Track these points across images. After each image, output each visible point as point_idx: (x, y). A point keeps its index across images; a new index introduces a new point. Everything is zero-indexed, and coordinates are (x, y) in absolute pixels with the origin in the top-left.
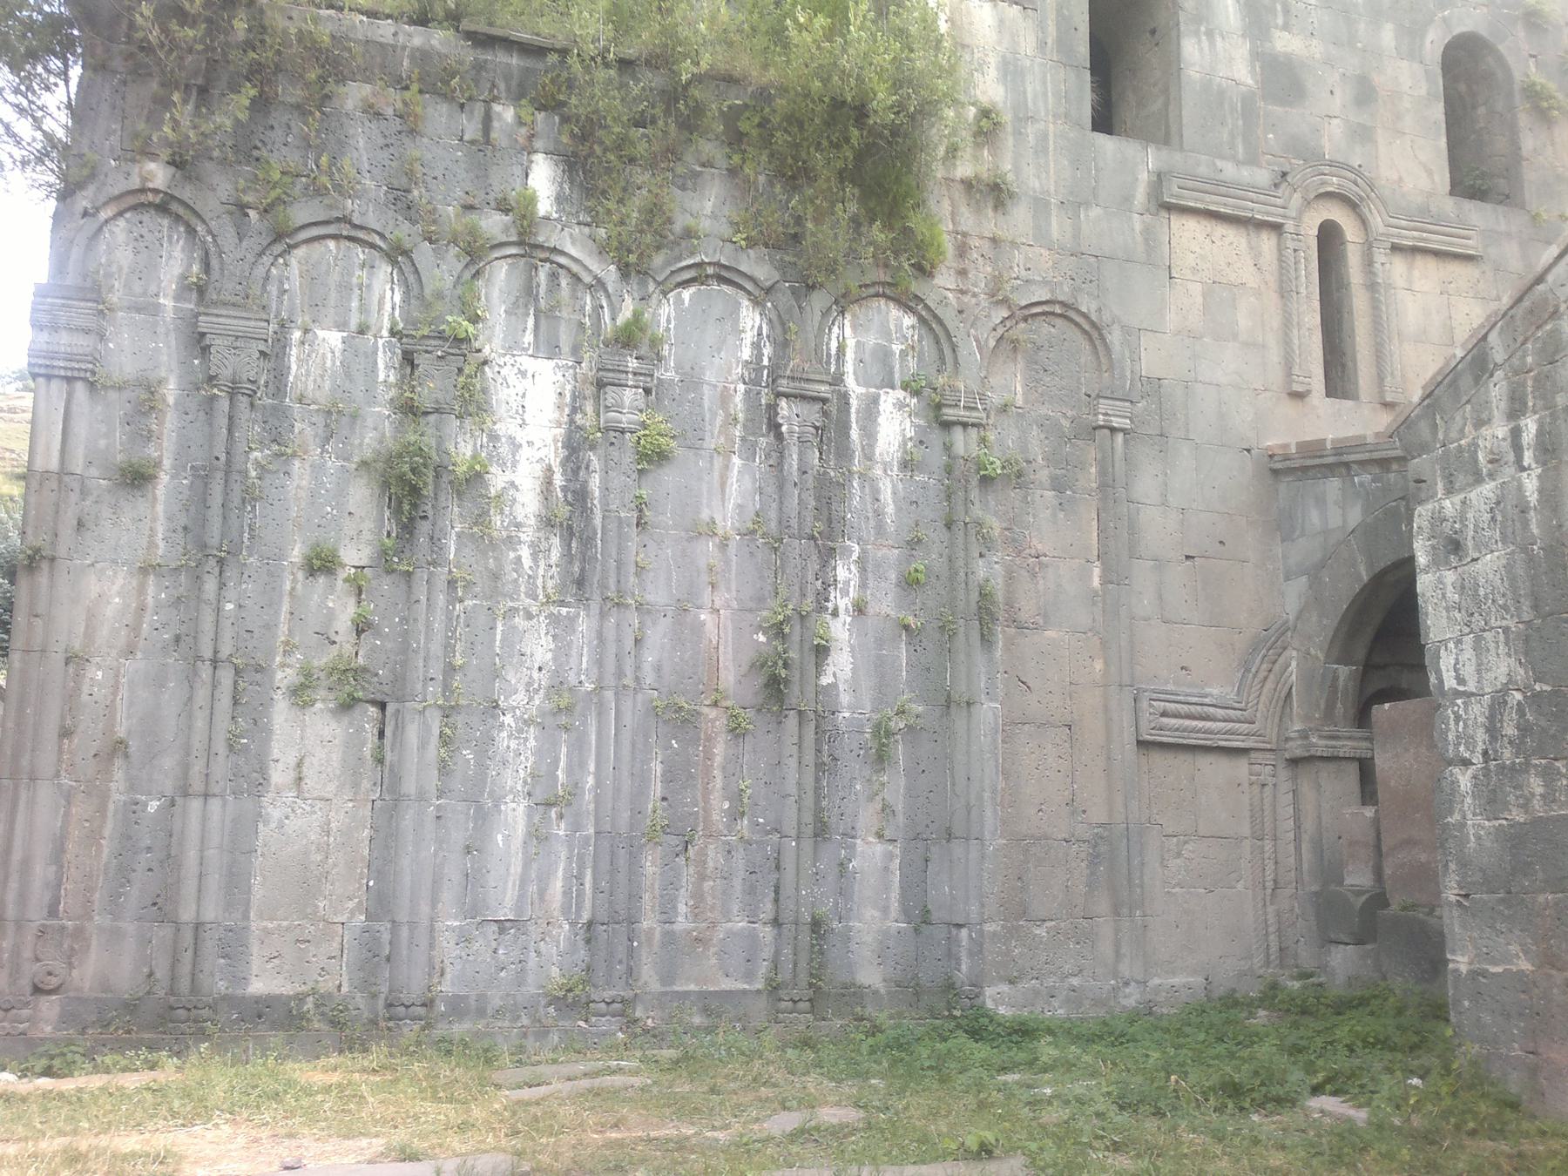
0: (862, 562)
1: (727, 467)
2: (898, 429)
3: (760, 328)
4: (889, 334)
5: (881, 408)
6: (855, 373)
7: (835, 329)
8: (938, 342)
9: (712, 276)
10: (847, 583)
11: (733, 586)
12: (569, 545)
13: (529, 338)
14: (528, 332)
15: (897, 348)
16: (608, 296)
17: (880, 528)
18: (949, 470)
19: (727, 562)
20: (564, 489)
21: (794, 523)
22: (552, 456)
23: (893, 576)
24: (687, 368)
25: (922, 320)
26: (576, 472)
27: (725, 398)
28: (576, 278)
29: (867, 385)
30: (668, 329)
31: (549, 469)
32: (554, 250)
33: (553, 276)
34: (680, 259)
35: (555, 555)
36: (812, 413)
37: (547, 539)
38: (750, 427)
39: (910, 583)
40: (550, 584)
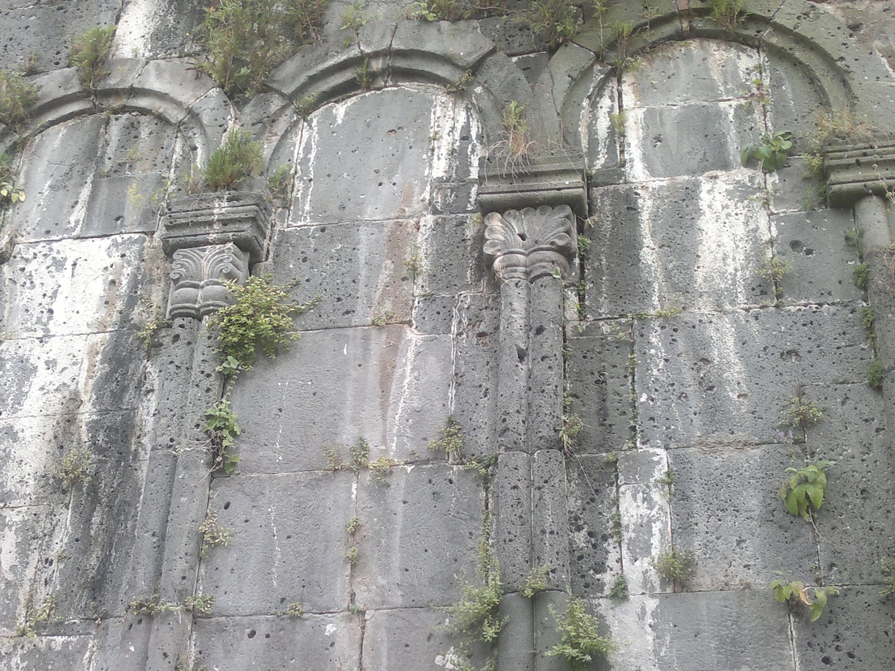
0: (677, 485)
1: (394, 349)
2: (741, 230)
3: (467, 128)
4: (713, 88)
5: (703, 204)
6: (646, 158)
7: (605, 102)
8: (812, 80)
9: (383, 73)
10: (645, 527)
11: (396, 561)
12: (88, 522)
13: (79, 213)
14: (79, 206)
15: (729, 107)
16: (204, 133)
17: (714, 412)
18: (863, 282)
19: (387, 517)
20: (94, 427)
21: (515, 421)
22: (82, 380)
23: (753, 501)
24: (334, 210)
25: (777, 54)
26: (117, 397)
27: (397, 239)
28: (162, 119)
29: (670, 172)
30: (305, 160)
31: (75, 399)
32: (134, 92)
33: (132, 128)
34: (326, 56)
35: (60, 541)
36: (552, 227)
37: (52, 514)
38: (443, 275)
39: (797, 512)
40: (43, 593)
